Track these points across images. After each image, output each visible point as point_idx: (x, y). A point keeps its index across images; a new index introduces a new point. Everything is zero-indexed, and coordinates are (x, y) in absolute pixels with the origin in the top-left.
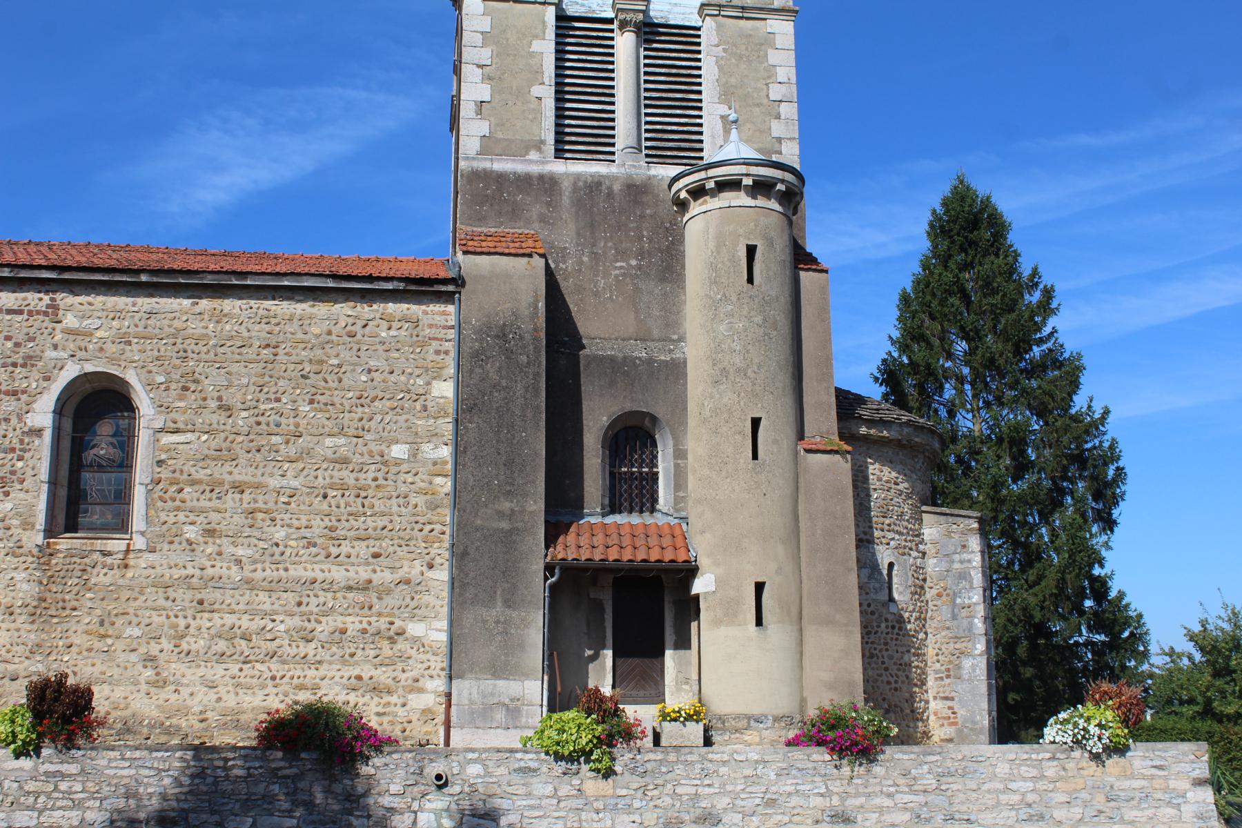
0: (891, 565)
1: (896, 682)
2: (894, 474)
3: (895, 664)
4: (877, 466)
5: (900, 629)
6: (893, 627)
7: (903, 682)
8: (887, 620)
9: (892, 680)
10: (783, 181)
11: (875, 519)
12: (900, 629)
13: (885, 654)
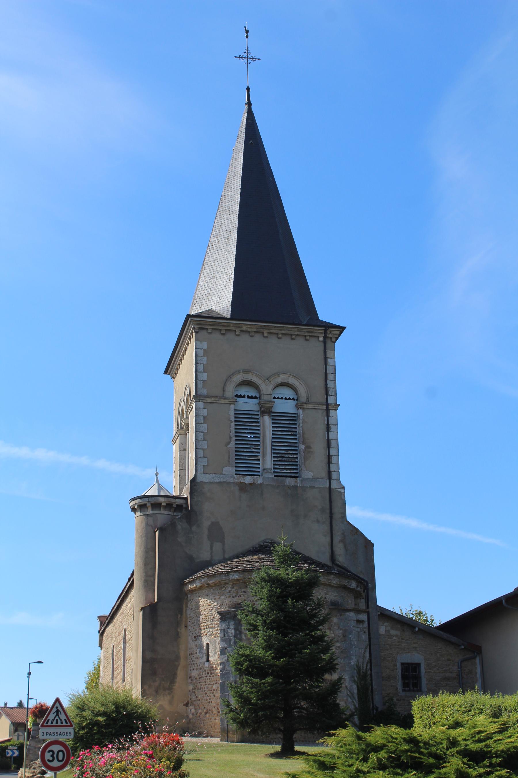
0: (208, 644)
1: (210, 699)
2: (208, 601)
3: (209, 690)
4: (203, 600)
5: (211, 674)
6: (208, 673)
7: (213, 699)
8: (205, 671)
9: (208, 698)
10: (136, 504)
11: (202, 625)
12: (211, 674)
13: (205, 686)
